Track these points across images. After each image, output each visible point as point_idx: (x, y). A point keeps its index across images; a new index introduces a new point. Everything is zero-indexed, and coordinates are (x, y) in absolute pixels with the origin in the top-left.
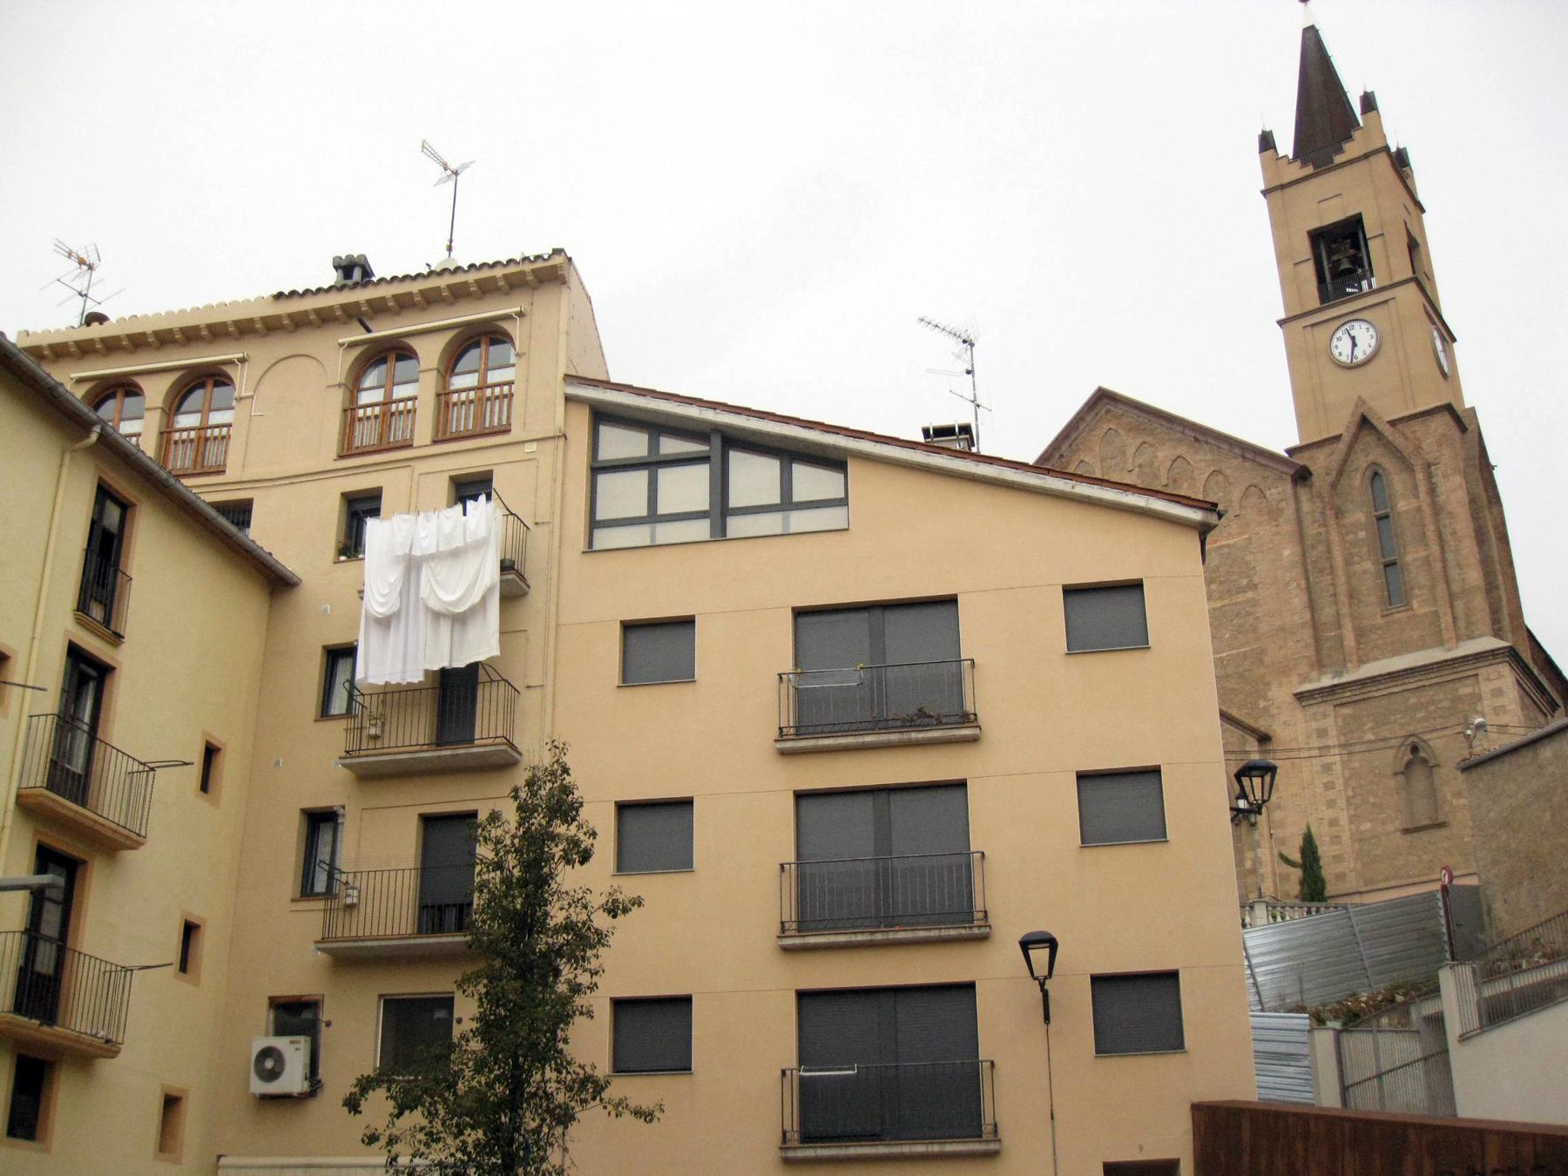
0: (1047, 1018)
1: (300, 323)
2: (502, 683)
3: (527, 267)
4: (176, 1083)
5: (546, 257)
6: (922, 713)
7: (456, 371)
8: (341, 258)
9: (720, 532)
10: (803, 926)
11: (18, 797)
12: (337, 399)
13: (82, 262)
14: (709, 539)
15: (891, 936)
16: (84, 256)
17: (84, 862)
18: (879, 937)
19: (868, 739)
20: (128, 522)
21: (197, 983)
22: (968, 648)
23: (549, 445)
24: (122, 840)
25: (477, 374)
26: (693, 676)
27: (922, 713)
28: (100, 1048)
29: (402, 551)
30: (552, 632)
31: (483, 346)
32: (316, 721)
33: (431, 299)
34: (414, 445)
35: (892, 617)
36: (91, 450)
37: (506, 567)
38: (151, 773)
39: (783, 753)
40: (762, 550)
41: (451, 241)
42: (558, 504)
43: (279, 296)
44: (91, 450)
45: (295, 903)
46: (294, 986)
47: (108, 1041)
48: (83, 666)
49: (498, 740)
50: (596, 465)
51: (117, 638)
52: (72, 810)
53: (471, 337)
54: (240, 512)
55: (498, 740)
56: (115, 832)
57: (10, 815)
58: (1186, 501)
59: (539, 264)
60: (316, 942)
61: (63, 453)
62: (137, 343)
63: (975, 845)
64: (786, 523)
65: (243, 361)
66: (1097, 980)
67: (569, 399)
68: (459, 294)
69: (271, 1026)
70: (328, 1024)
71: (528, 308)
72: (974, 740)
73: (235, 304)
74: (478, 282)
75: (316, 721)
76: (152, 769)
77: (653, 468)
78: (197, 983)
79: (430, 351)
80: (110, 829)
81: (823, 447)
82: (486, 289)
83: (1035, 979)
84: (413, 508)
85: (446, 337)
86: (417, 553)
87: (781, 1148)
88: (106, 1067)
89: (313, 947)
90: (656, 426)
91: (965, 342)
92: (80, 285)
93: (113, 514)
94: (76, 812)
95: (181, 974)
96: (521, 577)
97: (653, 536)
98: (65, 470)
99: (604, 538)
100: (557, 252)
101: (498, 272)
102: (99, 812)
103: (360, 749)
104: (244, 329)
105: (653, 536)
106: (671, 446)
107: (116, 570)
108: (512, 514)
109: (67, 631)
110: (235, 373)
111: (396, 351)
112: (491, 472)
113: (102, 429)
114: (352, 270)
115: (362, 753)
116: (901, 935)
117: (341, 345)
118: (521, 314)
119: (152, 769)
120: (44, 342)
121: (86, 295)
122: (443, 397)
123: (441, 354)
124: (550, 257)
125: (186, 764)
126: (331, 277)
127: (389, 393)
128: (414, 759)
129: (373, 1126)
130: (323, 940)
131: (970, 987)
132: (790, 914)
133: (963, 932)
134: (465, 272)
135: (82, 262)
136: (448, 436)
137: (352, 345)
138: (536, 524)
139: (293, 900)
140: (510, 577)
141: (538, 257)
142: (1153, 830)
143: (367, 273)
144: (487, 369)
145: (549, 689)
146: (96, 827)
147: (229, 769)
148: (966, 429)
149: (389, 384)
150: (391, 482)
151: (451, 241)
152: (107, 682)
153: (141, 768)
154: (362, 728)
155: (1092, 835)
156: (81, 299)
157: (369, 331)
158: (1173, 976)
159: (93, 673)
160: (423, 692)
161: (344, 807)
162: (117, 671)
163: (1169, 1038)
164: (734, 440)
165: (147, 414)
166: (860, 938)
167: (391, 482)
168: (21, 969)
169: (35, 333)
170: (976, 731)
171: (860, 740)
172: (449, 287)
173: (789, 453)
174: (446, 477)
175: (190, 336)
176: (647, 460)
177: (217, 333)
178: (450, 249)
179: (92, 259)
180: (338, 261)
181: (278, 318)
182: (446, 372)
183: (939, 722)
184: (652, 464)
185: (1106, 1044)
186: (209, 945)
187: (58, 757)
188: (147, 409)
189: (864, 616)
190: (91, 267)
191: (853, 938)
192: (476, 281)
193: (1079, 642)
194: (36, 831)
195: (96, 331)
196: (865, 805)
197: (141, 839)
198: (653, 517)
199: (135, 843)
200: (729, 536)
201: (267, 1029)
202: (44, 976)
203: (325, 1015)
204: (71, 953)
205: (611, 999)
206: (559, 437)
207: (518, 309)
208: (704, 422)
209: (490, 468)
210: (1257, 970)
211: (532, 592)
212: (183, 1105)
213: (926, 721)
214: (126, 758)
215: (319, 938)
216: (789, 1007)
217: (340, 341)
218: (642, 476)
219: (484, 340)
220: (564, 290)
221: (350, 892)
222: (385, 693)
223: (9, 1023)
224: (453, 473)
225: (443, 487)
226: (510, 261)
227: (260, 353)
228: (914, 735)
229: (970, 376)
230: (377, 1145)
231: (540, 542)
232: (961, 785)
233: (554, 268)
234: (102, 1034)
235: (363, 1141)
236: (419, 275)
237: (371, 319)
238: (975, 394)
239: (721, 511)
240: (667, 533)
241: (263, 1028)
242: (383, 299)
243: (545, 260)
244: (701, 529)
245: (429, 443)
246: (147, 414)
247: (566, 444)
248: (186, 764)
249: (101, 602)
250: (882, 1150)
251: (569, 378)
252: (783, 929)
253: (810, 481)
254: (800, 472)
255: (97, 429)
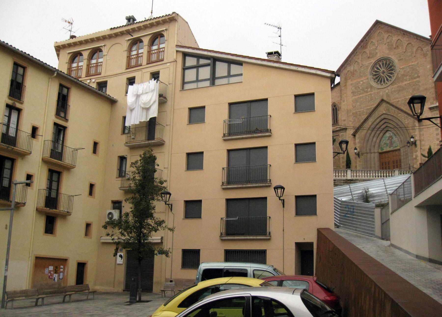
0: (284, 207)
1: (116, 35)
2: (159, 125)
3: (167, 17)
4: (89, 221)
5: (171, 14)
6: (257, 129)
7: (154, 45)
8: (127, 17)
9: (213, 83)
10: (229, 183)
11: (42, 159)
12: (125, 54)
13: (69, 23)
14: (209, 86)
15: (247, 186)
16: (70, 21)
17: (62, 172)
18: (244, 186)
19: (244, 136)
20: (69, 93)
21: (94, 198)
22: (270, 112)
23: (173, 63)
24: (70, 167)
25: (157, 46)
26: (204, 121)
27: (257, 129)
28: (66, 214)
29: (135, 93)
30: (172, 111)
31: (159, 38)
32: (121, 135)
33: (146, 27)
34: (143, 65)
35: (253, 104)
36: (56, 77)
37: (160, 96)
38: (77, 151)
39: (225, 140)
40: (222, 88)
41: (152, 11)
42: (174, 79)
43: (111, 29)
44: (56, 77)
45: (117, 179)
46: (116, 199)
47: (68, 212)
48: (59, 127)
49: (158, 139)
50: (185, 68)
51: (67, 120)
52: (55, 161)
53: (156, 36)
54: (103, 85)
55: (158, 139)
56: (67, 165)
57: (41, 163)
58: (326, 71)
59: (170, 17)
60: (119, 188)
61: (49, 78)
62: (81, 43)
63: (269, 163)
64: (229, 81)
65: (104, 46)
66: (297, 197)
67: (177, 51)
68: (152, 25)
69: (112, 207)
70: (124, 207)
71: (168, 28)
72: (270, 136)
73: (102, 31)
74: (156, 22)
75: (121, 135)
76: (77, 150)
77: (198, 68)
78: (94, 198)
79: (146, 41)
80: (66, 165)
81: (236, 60)
82: (158, 24)
83: (278, 197)
84: (142, 82)
85: (150, 37)
86: (139, 94)
87: (220, 237)
88: (69, 217)
89: (118, 189)
90: (199, 57)
91: (278, 28)
92: (69, 28)
93: (65, 91)
94: (56, 162)
95: (90, 196)
96: (165, 98)
97: (197, 86)
98: (50, 83)
99: (187, 87)
100: (174, 13)
101: (160, 19)
102: (64, 162)
103: (130, 142)
104: (104, 38)
105: (197, 86)
106: (202, 61)
107: (67, 105)
108: (162, 82)
109: (53, 120)
110: (103, 49)
111: (137, 41)
112: (159, 71)
113: (57, 72)
114: (131, 19)
115: (130, 143)
116: (249, 185)
117: (126, 40)
118: (166, 30)
119: (77, 150)
120: (60, 44)
121: (71, 31)
122: (150, 53)
123: (149, 41)
124: (172, 14)
125: (83, 149)
126: (125, 22)
127: (138, 52)
128: (140, 144)
129: (108, 232)
130: (121, 187)
131: (266, 198)
132: (225, 180)
133: (264, 185)
134: (153, 20)
135: (69, 23)
136: (150, 62)
137: (129, 40)
138: (169, 84)
139: (116, 178)
140: (161, 98)
141: (169, 15)
142: (312, 159)
143: (134, 20)
144: (160, 44)
145: (171, 126)
146: (62, 165)
147: (101, 148)
148: (277, 53)
149: (138, 50)
150: (137, 75)
151: (152, 11)
152: (66, 131)
153: (74, 150)
154: (130, 136)
155: (298, 160)
156: (70, 32)
157: (132, 36)
158: (315, 196)
159: (62, 128)
160: (144, 127)
161: (127, 155)
162: (68, 128)
163: (312, 212)
164: (215, 60)
165: (84, 61)
166: (240, 186)
167: (137, 75)
168: (46, 197)
169: (59, 42)
170: (270, 134)
171: (242, 136)
172: (149, 24)
173: (230, 62)
174: (149, 73)
175: (92, 40)
176: (197, 66)
177: (98, 39)
178: (152, 13)
179: (72, 22)
180: (127, 18)
181: (111, 34)
182: (150, 45)
183: (261, 132)
184: (197, 67)
185: (298, 213)
186: (97, 190)
187: (54, 149)
188: (84, 59)
189: (246, 104)
190: (72, 24)
191: (238, 186)
192: (155, 22)
193: (298, 110)
194: (48, 166)
195: (74, 40)
196: (244, 153)
197: (74, 166)
198: (197, 81)
199: (73, 167)
200: (216, 85)
201: (111, 208)
202: (53, 198)
203: (123, 205)
204: (60, 194)
205: (184, 201)
206: (174, 61)
207: (165, 28)
208: (208, 55)
209: (159, 70)
210: (387, 189)
211: (168, 102)
212: (91, 226)
213: (258, 131)
214: (71, 149)
215: (120, 187)
216: (224, 203)
217: (126, 39)
218: (195, 70)
219: (159, 37)
220: (176, 22)
221: (128, 176)
222: (136, 128)
223: (42, 209)
224: (151, 72)
225: (148, 75)
226: (163, 16)
227: (108, 43)
228: (255, 135)
229: (280, 37)
230: (109, 236)
231: (170, 88)
232: (266, 147)
233: (173, 17)
234: (66, 211)
235: (106, 235)
236: (142, 21)
237: (133, 33)
238: (281, 42)
239: (213, 79)
240: (201, 84)
241: (110, 207)
242: (134, 28)
243: (171, 15)
244: (208, 83)
245: (145, 64)
246: (84, 61)
247: (176, 64)
248: (83, 149)
249: (63, 112)
250: (243, 238)
251: (177, 46)
252: (223, 184)
253: (235, 69)
254: (233, 66)
255: (56, 73)
